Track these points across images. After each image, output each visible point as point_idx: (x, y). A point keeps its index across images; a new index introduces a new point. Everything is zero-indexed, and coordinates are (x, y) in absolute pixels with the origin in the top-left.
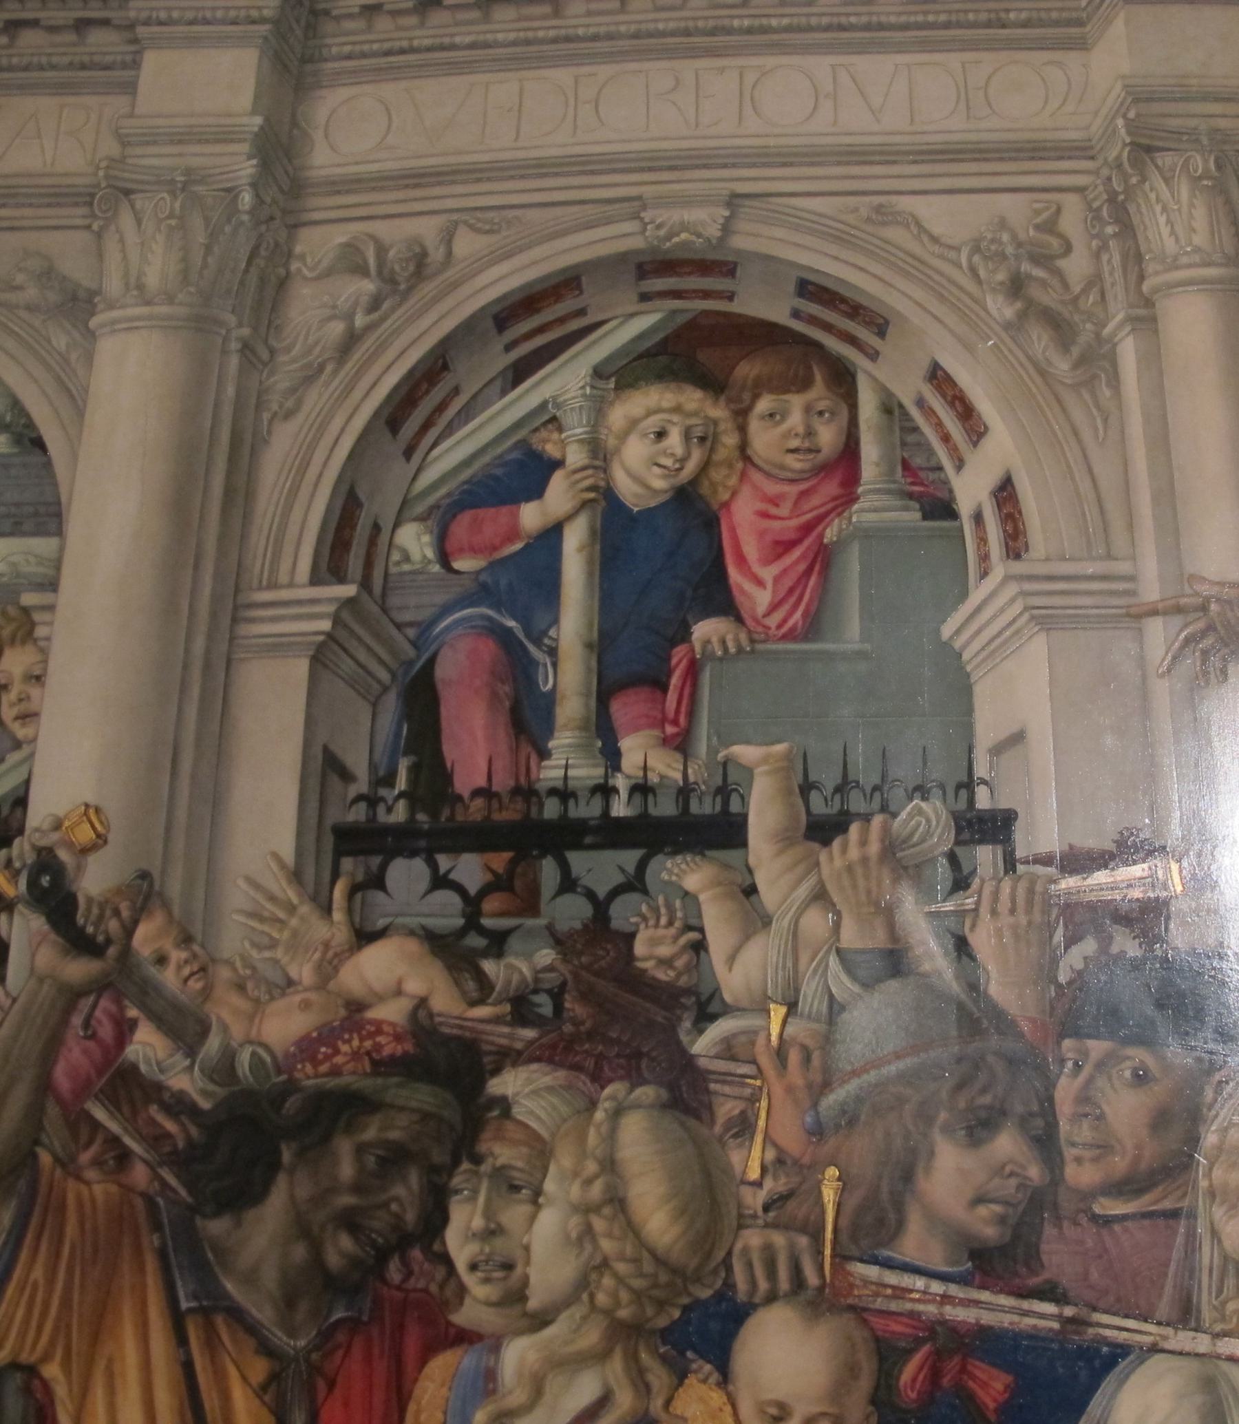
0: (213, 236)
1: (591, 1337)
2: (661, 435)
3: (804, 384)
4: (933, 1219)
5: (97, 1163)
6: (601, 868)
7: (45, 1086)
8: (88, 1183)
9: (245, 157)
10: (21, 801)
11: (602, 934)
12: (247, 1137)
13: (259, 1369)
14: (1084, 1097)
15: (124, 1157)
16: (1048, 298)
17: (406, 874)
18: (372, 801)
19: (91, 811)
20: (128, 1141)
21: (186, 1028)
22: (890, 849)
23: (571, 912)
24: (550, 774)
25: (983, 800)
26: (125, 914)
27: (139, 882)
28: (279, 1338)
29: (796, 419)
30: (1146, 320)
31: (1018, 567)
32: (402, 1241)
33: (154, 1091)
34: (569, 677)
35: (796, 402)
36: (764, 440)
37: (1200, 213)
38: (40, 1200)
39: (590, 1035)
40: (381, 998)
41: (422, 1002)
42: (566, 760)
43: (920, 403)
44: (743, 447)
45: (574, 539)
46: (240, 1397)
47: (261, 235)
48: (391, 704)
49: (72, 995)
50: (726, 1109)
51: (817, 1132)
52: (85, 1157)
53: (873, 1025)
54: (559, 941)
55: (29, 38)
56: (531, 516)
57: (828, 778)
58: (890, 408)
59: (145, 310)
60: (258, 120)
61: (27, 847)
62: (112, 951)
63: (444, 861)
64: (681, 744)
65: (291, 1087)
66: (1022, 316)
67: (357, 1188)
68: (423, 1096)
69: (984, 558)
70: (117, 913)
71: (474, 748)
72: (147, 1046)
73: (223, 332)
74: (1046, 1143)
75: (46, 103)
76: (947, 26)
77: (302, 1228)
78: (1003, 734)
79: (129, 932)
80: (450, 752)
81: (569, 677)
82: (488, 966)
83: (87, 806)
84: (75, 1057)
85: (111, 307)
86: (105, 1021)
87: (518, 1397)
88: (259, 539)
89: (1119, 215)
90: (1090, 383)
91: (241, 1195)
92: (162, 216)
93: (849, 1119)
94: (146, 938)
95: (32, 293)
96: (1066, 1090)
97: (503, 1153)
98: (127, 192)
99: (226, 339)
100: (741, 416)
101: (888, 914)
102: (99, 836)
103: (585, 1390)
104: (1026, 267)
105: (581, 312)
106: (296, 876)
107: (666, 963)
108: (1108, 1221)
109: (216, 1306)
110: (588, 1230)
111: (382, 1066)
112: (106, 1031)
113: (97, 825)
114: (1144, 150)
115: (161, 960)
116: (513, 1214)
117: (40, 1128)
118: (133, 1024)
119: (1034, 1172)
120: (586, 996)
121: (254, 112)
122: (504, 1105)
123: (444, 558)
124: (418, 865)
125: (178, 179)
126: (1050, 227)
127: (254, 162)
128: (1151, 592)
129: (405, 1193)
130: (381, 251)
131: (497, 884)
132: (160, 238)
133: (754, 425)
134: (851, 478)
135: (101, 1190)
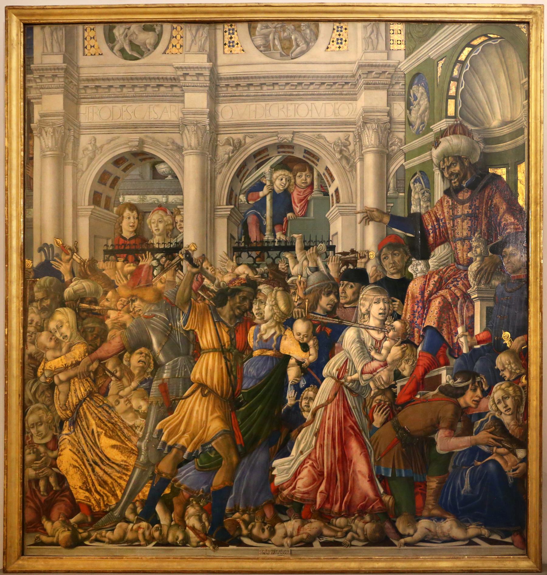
1: (273, 324)
2: (282, 179)
3: (305, 171)
4: (322, 308)
6: (274, 254)
7: (191, 288)
10: (182, 242)
11: (274, 265)
12: (223, 295)
13: (227, 329)
14: (343, 290)
15: (204, 299)
16: (346, 154)
17: (244, 255)
18: (239, 243)
21: (212, 279)
22: (317, 251)
23: (269, 261)
24: (266, 238)
25: (331, 244)
28: (229, 325)
29: (303, 177)
30: (362, 159)
31: (338, 205)
32: (246, 311)
33: (208, 289)
34: (268, 222)
35: (304, 173)
36: (298, 181)
37: (373, 137)
39: (273, 280)
40: (241, 274)
41: (248, 275)
42: (268, 236)
43: (324, 174)
44: (295, 182)
45: (268, 198)
46: (224, 334)
48: (240, 226)
49: (194, 274)
50: (292, 291)
51: (305, 294)
53: (314, 278)
54: (267, 265)
55: (162, 89)
56: (261, 194)
57: (308, 240)
58: (319, 175)
63: (250, 253)
64: (285, 234)
65: (229, 288)
66: (341, 157)
67: (239, 303)
68: (248, 289)
69: (333, 203)
71: (254, 235)
72: (206, 282)
74: (338, 297)
75: (167, 105)
76: (332, 95)
77: (232, 309)
78: (335, 232)
79: (202, 264)
80: (250, 235)
81: (268, 222)
82: (257, 269)
84: (195, 285)
87: (263, 332)
88: (217, 197)
89: (359, 137)
90: (352, 171)
91: (222, 304)
93: (310, 292)
94: (205, 265)
95: (171, 147)
96: (341, 289)
97: (260, 298)
100: (295, 176)
101: (316, 261)
103: (272, 331)
104: (343, 148)
105: (268, 155)
106: (227, 255)
107: (283, 269)
108: (345, 308)
109: (220, 321)
110: (273, 309)
111: (242, 285)
112: (200, 280)
114: (365, 123)
116: (262, 306)
119: (336, 301)
120: (272, 274)
122: (260, 290)
123: (248, 201)
124: (246, 253)
126: (347, 140)
128: (358, 209)
129: (246, 304)
130: (233, 141)
131: (258, 256)
133: (297, 178)
134: (313, 188)
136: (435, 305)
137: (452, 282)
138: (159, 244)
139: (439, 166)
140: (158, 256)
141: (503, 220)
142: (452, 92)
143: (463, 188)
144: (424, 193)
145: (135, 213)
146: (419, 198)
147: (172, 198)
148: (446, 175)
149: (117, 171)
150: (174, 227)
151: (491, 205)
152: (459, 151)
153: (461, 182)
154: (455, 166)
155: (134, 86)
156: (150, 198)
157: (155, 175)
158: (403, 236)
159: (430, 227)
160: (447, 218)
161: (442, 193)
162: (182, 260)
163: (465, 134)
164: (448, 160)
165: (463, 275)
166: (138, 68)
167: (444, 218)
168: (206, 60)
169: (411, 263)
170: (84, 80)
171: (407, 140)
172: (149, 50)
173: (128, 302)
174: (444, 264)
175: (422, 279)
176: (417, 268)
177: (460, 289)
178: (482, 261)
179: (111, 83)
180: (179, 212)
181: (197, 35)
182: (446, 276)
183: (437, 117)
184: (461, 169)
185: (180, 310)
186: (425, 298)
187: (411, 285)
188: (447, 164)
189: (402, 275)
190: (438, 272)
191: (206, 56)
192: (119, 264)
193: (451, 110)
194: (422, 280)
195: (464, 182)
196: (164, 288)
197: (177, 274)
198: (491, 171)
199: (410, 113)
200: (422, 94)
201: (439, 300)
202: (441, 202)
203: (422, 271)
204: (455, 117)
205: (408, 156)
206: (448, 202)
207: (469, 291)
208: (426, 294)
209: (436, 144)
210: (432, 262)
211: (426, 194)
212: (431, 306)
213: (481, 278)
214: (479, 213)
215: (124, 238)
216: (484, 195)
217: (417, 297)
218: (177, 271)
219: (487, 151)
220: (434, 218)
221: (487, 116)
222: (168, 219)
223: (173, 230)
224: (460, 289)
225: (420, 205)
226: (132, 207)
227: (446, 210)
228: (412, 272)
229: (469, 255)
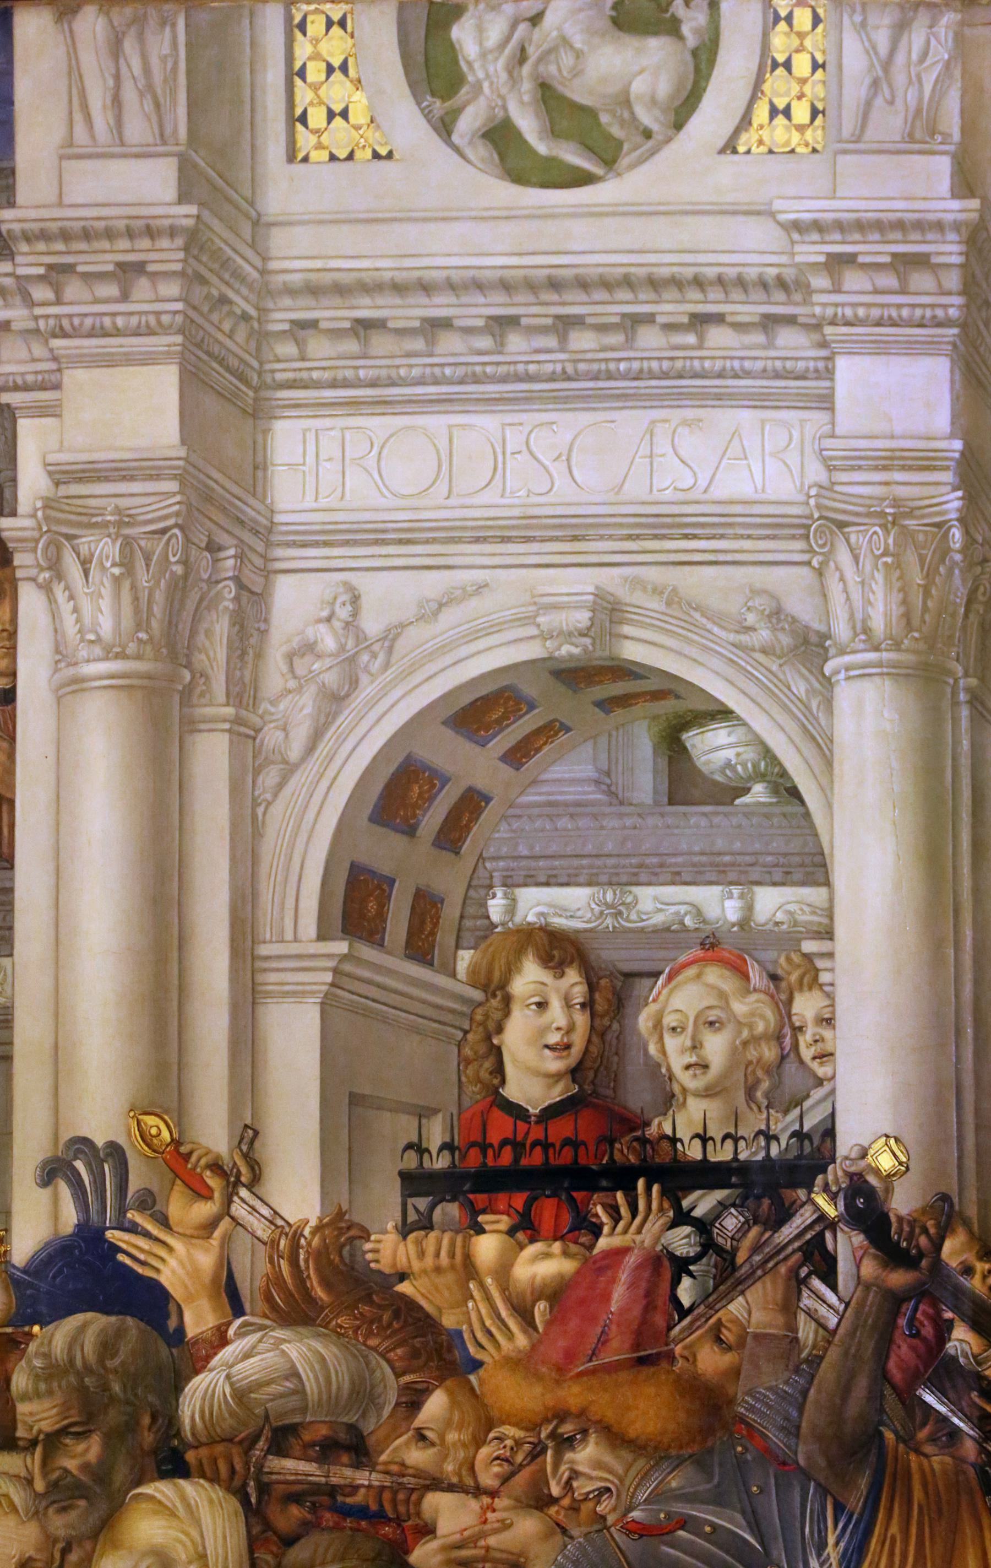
0: (930, 576)
5: (933, 1439)
7: (885, 1375)
8: (926, 1456)
9: (949, 488)
10: (830, 1133)
15: (955, 1433)
19: (892, 1141)
20: (956, 1421)
26: (932, 1231)
27: (940, 1203)
38: (889, 1470)
47: (976, 578)
49: (895, 1301)
52: (922, 1434)
55: (718, 336)
59: (872, 656)
60: (958, 445)
61: (840, 1173)
62: (924, 1263)
70: (925, 1231)
73: (951, 681)
75: (746, 417)
79: (938, 1247)
83: (887, 1136)
85: (842, 652)
86: (926, 1323)
92: (878, 553)
94: (953, 1250)
95: (764, 635)
98: (841, 525)
99: (954, 693)
102: (901, 1164)
112: (928, 1331)
113: (898, 1153)
115: (968, 1271)
117: (882, 1410)
118: (950, 1325)
121: (952, 436)
125: (888, 510)
127: (959, 494)
132: (879, 577)
135: (939, 1461)
138: (704, 1139)
140: (702, 1203)
145: (573, 976)
147: (772, 903)
149: (473, 764)
150: (788, 1054)
155: (565, 325)
156: (655, 903)
157: (682, 782)
162: (832, 1225)
166: (585, 228)
168: (944, 186)
170: (290, 291)
172: (648, 134)
173: (537, 1452)
179: (441, 306)
180: (811, 977)
181: (900, 58)
185: (824, 1491)
191: (943, 166)
192: (487, 1247)
196: (735, 1372)
197: (807, 1301)
215: (516, 1111)
218: (804, 1282)
222: (751, 1007)
223: (782, 1066)
226: (558, 948)
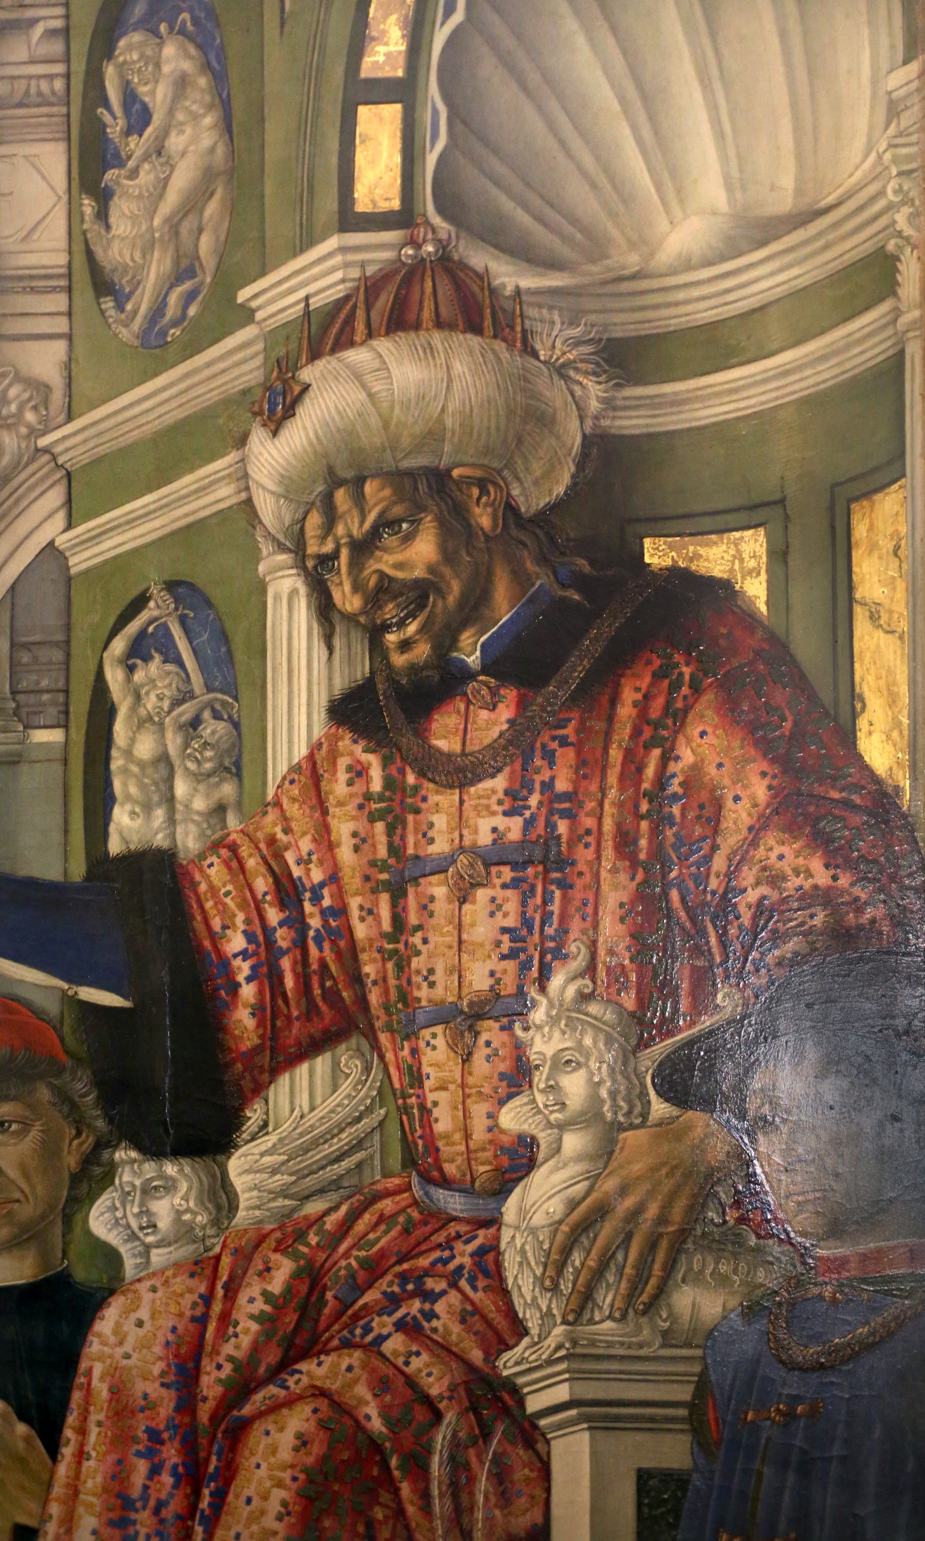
136: (276, 1452)
137: (393, 1301)
139: (296, 545)
141: (748, 876)
142: (386, 52)
143: (468, 675)
144: (195, 723)
146: (163, 759)
148: (347, 599)
151: (661, 781)
152: (433, 435)
153: (445, 640)
154: (409, 538)
158: (52, 1007)
159: (236, 942)
160: (352, 881)
161: (320, 716)
163: (476, 329)
164: (359, 499)
165: (464, 1255)
167: (334, 878)
169: (107, 1178)
171: (83, 385)
174: (335, 1184)
175: (180, 1283)
176: (145, 1210)
177: (444, 1350)
178: (605, 1152)
182: (348, 1260)
183: (279, 223)
184: (448, 556)
186: (204, 1412)
187: (107, 1322)
188: (353, 525)
189: (44, 1256)
190: (289, 1235)
193: (377, 176)
194: (188, 1290)
195: (466, 638)
198: (657, 554)
199: (102, 215)
200: (182, 83)
201: (298, 1420)
202: (312, 773)
203: (184, 1232)
204: (404, 218)
205: (85, 490)
206: (359, 772)
207: (508, 1364)
208: (212, 1382)
209: (278, 402)
210: (248, 1168)
211: (213, 729)
212: (247, 1460)
213: (599, 1273)
214: (575, 839)
216: (611, 719)
217: (149, 1405)
219: (631, 423)
220: (262, 884)
221: (625, 194)
224: (444, 1350)
225: (170, 799)
227: (343, 828)
228: (113, 1238)
229: (512, 1118)
